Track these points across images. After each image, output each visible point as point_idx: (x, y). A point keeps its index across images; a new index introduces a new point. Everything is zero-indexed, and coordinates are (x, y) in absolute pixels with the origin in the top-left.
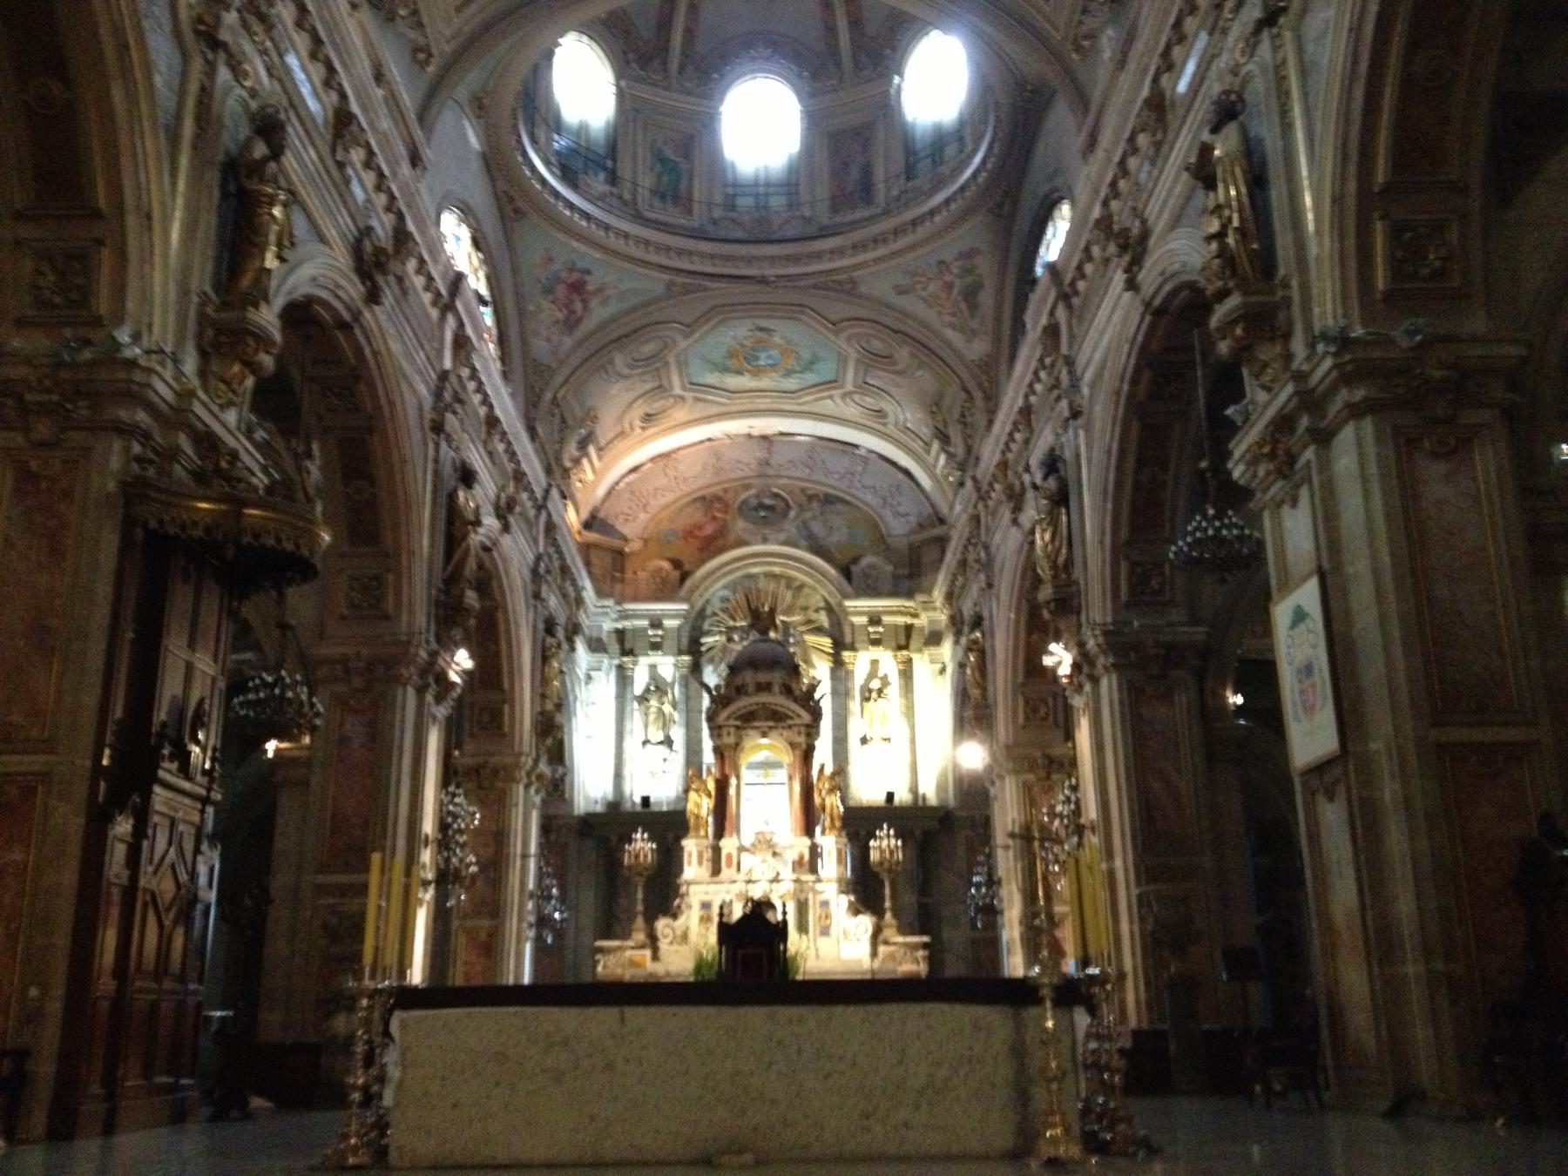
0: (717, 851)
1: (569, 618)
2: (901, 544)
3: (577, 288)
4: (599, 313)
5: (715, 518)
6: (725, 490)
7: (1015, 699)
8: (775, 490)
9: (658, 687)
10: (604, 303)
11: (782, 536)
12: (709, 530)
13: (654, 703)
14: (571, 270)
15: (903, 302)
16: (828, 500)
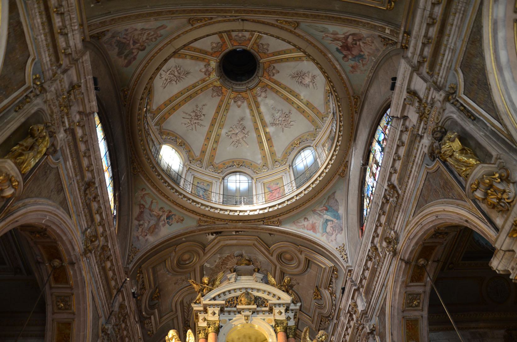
3: (346, 47)
10: (335, 34)
14: (345, 56)
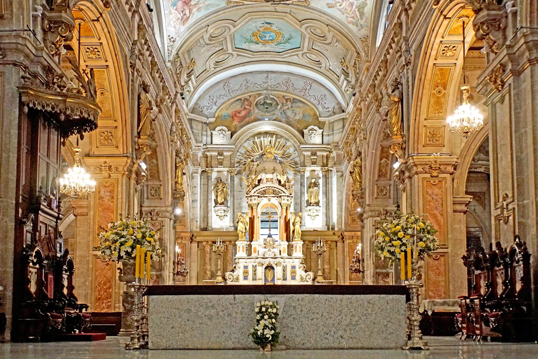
0: (250, 246)
5: (245, 109)
6: (250, 96)
7: (373, 187)
8: (271, 96)
12: (243, 113)
15: (330, 11)
16: (294, 101)
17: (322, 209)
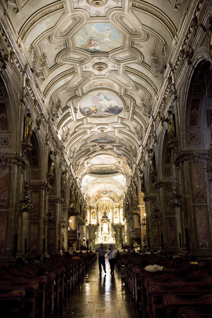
1: (65, 169)
2: (119, 196)
4: (89, 181)
9: (94, 212)
11: (106, 196)
12: (99, 195)
13: (93, 214)
16: (111, 191)
17: (118, 219)
